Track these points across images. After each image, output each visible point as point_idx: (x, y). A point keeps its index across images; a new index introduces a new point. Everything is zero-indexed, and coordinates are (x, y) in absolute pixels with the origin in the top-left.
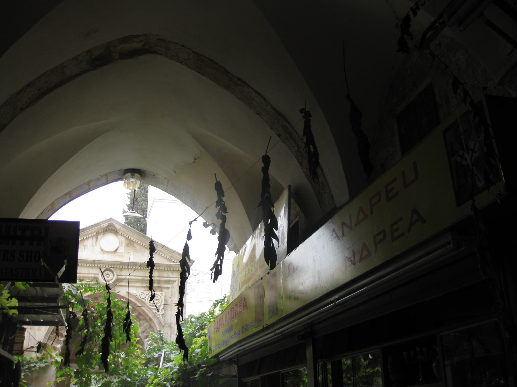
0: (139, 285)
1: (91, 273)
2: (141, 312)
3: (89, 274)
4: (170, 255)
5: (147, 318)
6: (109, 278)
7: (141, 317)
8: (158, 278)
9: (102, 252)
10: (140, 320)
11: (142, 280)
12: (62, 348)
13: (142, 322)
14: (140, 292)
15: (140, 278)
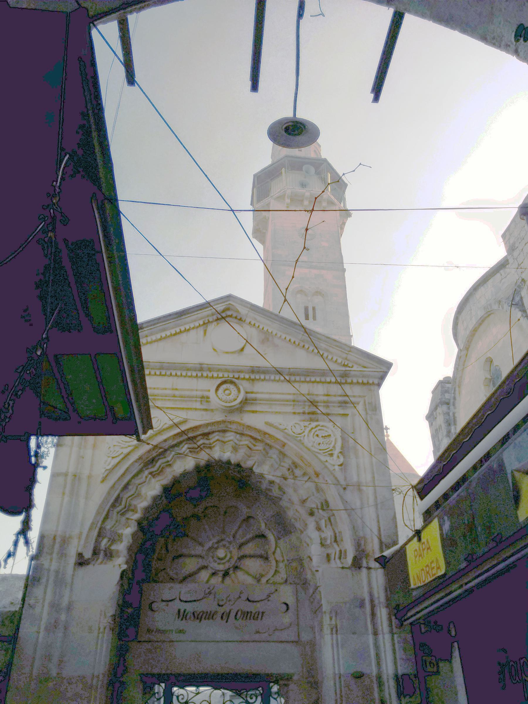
0: (289, 409)
2: (297, 460)
4: (344, 356)
5: (310, 471)
6: (231, 397)
7: (298, 472)
8: (325, 398)
10: (295, 478)
11: (294, 401)
12: (134, 535)
15: (291, 397)
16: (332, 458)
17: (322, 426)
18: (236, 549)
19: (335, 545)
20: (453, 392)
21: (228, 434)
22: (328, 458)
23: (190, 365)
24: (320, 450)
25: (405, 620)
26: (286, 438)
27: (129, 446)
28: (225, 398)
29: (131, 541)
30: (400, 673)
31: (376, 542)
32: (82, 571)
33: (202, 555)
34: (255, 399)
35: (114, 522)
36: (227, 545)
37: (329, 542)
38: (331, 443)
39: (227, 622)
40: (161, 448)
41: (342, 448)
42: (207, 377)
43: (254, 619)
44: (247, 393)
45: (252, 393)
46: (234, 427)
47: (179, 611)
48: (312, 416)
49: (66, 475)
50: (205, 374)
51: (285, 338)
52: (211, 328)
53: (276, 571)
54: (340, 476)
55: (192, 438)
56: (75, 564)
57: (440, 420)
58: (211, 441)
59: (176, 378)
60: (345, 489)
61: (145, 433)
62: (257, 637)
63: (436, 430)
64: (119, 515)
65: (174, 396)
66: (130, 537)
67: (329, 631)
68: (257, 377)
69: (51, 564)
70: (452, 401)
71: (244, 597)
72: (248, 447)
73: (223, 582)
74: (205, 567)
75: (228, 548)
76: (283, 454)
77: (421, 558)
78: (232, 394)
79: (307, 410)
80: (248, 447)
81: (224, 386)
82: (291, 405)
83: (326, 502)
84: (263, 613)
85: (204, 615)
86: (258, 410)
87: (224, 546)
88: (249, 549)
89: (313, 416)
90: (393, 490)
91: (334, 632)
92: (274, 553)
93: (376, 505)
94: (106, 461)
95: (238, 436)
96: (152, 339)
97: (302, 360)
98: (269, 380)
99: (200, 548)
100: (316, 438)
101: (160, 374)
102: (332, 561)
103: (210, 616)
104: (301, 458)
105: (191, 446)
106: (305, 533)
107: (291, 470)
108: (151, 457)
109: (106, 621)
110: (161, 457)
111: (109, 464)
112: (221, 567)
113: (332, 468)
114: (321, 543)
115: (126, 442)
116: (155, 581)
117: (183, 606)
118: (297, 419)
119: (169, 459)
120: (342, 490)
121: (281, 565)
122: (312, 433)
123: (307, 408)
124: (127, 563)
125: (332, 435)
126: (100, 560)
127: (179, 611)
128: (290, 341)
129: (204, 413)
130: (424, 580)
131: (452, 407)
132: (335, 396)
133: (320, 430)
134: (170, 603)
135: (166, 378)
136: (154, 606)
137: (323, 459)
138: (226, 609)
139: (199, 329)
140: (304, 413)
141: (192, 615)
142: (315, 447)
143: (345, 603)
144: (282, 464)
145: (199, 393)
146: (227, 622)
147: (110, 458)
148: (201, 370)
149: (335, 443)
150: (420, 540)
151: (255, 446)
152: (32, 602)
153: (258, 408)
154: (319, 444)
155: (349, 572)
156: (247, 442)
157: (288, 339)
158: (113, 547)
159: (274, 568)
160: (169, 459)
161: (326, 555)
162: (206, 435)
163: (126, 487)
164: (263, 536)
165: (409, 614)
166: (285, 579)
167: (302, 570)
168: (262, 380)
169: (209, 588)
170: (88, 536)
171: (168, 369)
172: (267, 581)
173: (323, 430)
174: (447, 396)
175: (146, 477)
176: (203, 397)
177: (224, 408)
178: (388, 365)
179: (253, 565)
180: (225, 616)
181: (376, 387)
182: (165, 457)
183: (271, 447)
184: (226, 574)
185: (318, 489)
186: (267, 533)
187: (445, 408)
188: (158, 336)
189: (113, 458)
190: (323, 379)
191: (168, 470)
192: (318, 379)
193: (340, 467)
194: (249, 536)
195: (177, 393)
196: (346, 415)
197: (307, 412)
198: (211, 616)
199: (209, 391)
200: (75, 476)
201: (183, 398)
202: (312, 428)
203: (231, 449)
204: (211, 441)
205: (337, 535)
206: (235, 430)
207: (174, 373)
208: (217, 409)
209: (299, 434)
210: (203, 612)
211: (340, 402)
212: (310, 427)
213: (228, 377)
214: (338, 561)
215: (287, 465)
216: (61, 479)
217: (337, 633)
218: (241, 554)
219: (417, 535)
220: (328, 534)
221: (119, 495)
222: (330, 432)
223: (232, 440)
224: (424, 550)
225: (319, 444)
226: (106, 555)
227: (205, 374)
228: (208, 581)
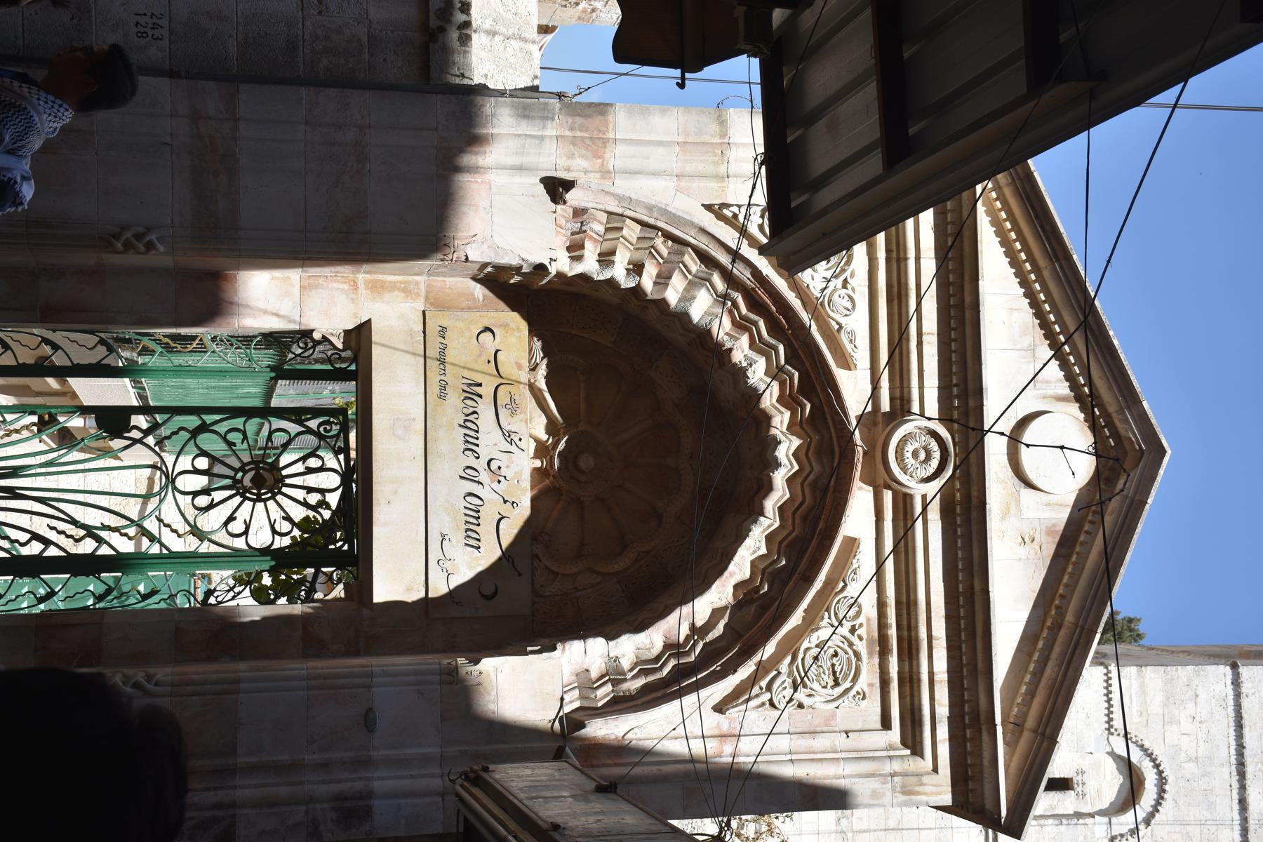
28: (910, 448)
30: (377, 804)
39: (461, 477)
43: (467, 530)
47: (480, 385)
81: (934, 446)
103: (471, 446)
117: (486, 391)
127: (480, 385)
138: (484, 476)
141: (472, 410)
146: (461, 477)
165: (476, 791)
172: (536, 556)
173: (849, 669)
180: (469, 474)
191: (745, 339)
202: (851, 644)
212: (855, 640)
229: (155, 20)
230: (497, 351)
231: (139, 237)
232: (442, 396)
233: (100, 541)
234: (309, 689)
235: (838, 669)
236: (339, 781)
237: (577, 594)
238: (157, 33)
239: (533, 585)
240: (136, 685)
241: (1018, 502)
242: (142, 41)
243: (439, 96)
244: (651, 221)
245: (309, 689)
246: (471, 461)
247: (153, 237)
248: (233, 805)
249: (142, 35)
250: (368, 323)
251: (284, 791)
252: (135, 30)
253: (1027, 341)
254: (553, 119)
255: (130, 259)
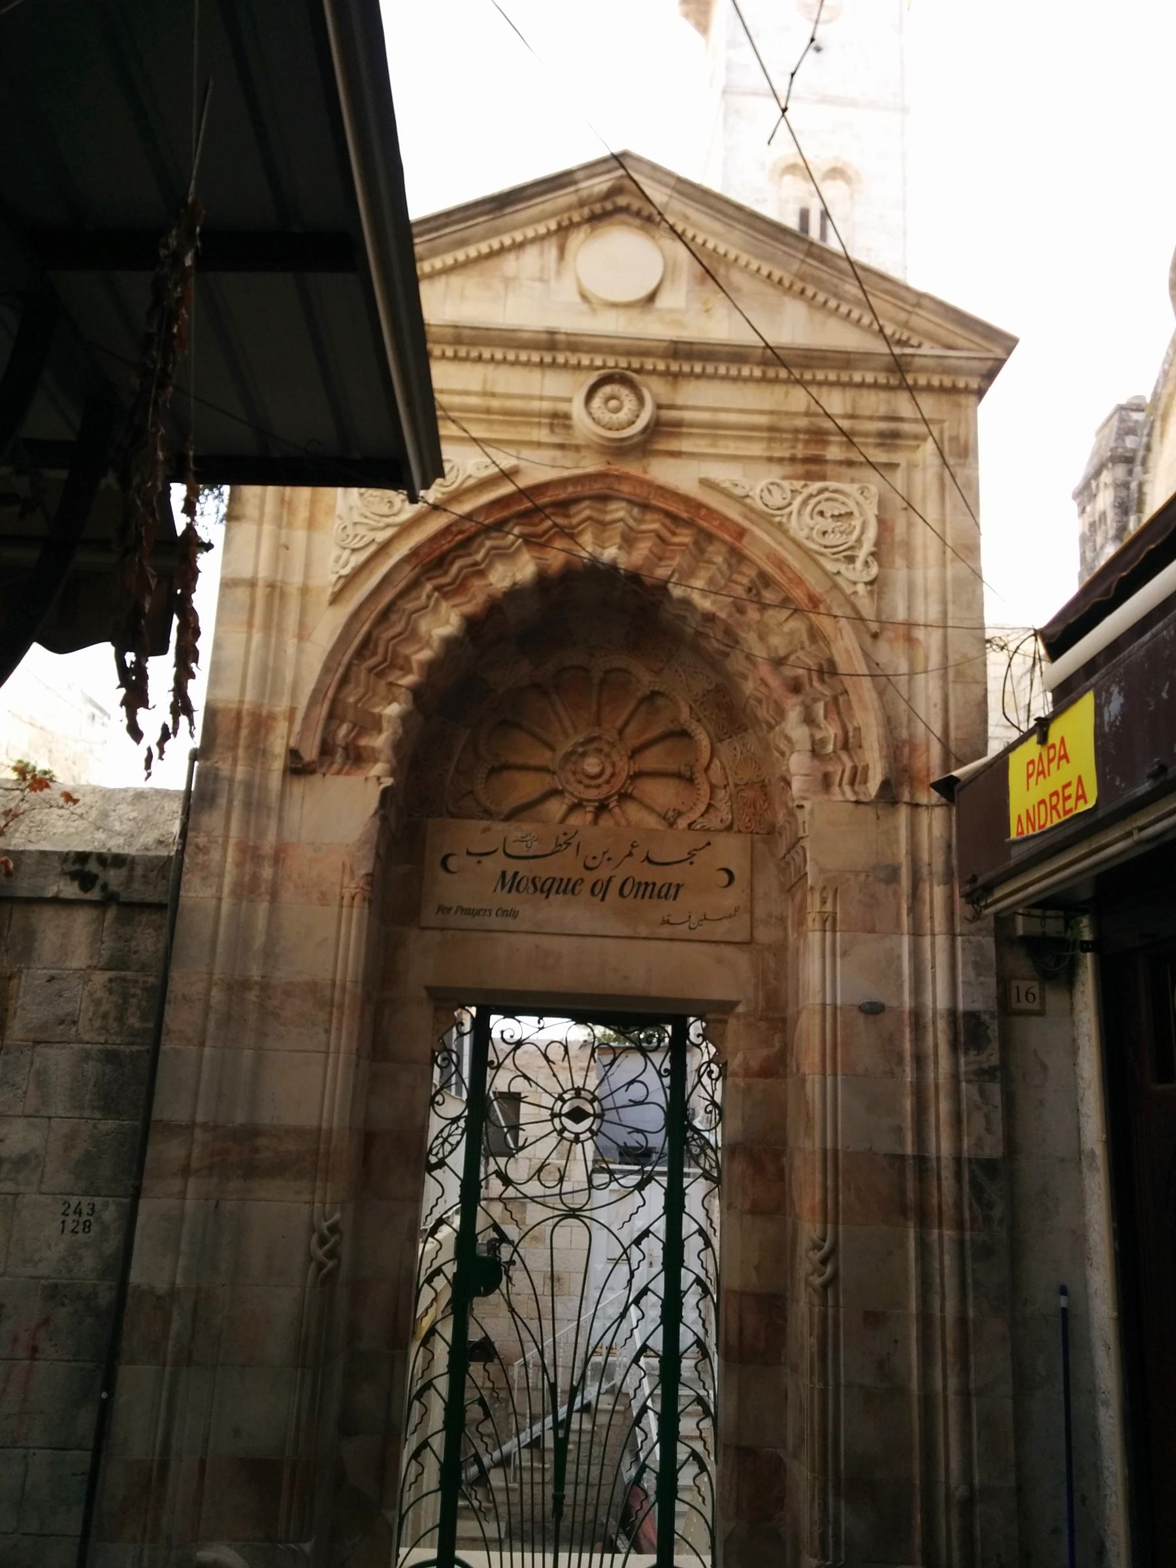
0: (757, 449)
1: (536, 391)
2: (770, 569)
3: (530, 397)
4: (903, 316)
5: (799, 595)
6: (623, 416)
7: (769, 596)
9: (584, 307)
11: (772, 429)
13: (775, 616)
14: (763, 483)
15: (762, 420)
16: (851, 566)
17: (835, 491)
18: (625, 758)
19: (844, 757)
20: (1146, 432)
21: (613, 506)
22: (842, 567)
23: (526, 336)
24: (825, 547)
25: (987, 906)
26: (746, 517)
27: (388, 526)
28: (607, 417)
29: (400, 731)
31: (936, 749)
32: (298, 787)
33: (551, 767)
34: (679, 424)
35: (361, 690)
36: (606, 749)
37: (830, 748)
38: (851, 533)
39: (603, 899)
40: (461, 532)
41: (877, 543)
42: (565, 366)
44: (659, 407)
45: (672, 407)
46: (626, 488)
47: (504, 873)
48: (812, 467)
49: (252, 584)
50: (561, 359)
51: (759, 270)
52: (576, 239)
53: (710, 805)
54: (867, 608)
55: (531, 511)
56: (285, 771)
57: (1105, 500)
58: (575, 521)
59: (491, 367)
60: (875, 636)
61: (427, 486)
62: (665, 931)
63: (1093, 526)
64: (372, 676)
65: (488, 411)
66: (399, 721)
67: (818, 926)
68: (686, 368)
69: (235, 769)
70: (1141, 454)
71: (639, 854)
72: (659, 537)
73: (595, 821)
74: (555, 793)
75: (608, 756)
76: (737, 556)
77: (1041, 777)
78: (625, 410)
79: (800, 451)
80: (659, 537)
81: (607, 390)
82: (760, 439)
83: (831, 662)
84: (679, 886)
85: (556, 885)
86: (684, 449)
87: (600, 751)
88: (652, 759)
89: (814, 468)
90: (988, 641)
91: (828, 925)
92: (707, 769)
93: (945, 668)
94: (339, 557)
95: (636, 511)
96: (433, 267)
97: (793, 326)
98: (714, 377)
99: (548, 754)
100: (819, 519)
101: (455, 358)
102: (836, 789)
103: (568, 887)
104: (781, 564)
105: (528, 530)
106: (777, 728)
107: (754, 591)
108: (437, 553)
109: (353, 886)
110: (461, 552)
111: (347, 563)
112: (593, 794)
113: (849, 590)
114: (813, 751)
115: (382, 516)
116: (452, 815)
117: (512, 866)
118: (775, 473)
119: (479, 557)
120: (868, 640)
121: (721, 794)
122: (809, 508)
123: (800, 446)
124: (392, 773)
125: (856, 513)
126: (336, 767)
127: (504, 873)
128: (769, 276)
129: (558, 453)
130: (1042, 823)
131: (1138, 469)
132: (871, 418)
133: (827, 500)
134: (483, 859)
135: (468, 366)
136: (452, 863)
137: (831, 567)
138: (603, 874)
139: (546, 243)
140: (793, 460)
141: (530, 884)
142: (813, 541)
143: (857, 874)
144: (736, 577)
145: (546, 406)
146: (603, 899)
147: (347, 552)
148: (551, 348)
149: (862, 533)
150: (1043, 740)
151: (674, 534)
152: (202, 840)
153: (686, 445)
154: (825, 533)
155: (869, 813)
156: (655, 526)
157: (764, 272)
158: (363, 742)
159: (706, 800)
160: (479, 557)
161: (820, 776)
162: (563, 506)
163: (384, 616)
164: (684, 734)
165: (998, 894)
166: (728, 823)
167: (765, 806)
168: (699, 377)
169: (565, 834)
170: (306, 717)
171: (473, 343)
172: (690, 825)
174: (1130, 442)
175: (429, 597)
176: (555, 415)
177: (607, 443)
178: (1008, 343)
179: (663, 793)
180: (600, 890)
181: (973, 399)
182: (470, 555)
183: (710, 537)
184: (602, 807)
185: (814, 634)
186: (693, 727)
187: (1120, 471)
188: (449, 259)
189: (354, 550)
190: (845, 377)
191: (477, 583)
192: (832, 377)
193: (869, 588)
194: (655, 732)
195: (495, 403)
196: (892, 466)
197: (800, 456)
198: (570, 887)
199: (570, 400)
200: (272, 586)
201: (511, 416)
202: (811, 496)
203: (618, 540)
204: (575, 521)
205: (851, 734)
206: (627, 497)
207: (487, 354)
208: (588, 447)
209: (779, 509)
210: (554, 879)
211: (882, 434)
213: (616, 366)
214: (847, 788)
215: (745, 581)
216: (242, 594)
217: (834, 930)
218: (634, 767)
219: (1038, 729)
220: (831, 731)
221: (369, 635)
222: (853, 507)
223: (621, 520)
224: (1050, 761)
225: (825, 533)
226: (347, 757)
227: (561, 359)
228: (563, 820)
229: (71, 1211)
230: (469, 853)
231: (322, 1241)
232: (514, 914)
233: (645, 1291)
234: (835, 1074)
235: (836, 513)
236: (936, 1046)
237: (731, 785)
238: (86, 1210)
239: (721, 831)
240: (824, 1262)
241: (671, 311)
242: (94, 1228)
243: (181, 893)
244: (341, 670)
245: (835, 1074)
246: (587, 887)
247: (325, 1225)
248: (958, 1160)
249: (87, 1226)
250: (427, 988)
251: (944, 1106)
252: (81, 1235)
253: (498, 286)
254: (217, 769)
255: (345, 1251)
